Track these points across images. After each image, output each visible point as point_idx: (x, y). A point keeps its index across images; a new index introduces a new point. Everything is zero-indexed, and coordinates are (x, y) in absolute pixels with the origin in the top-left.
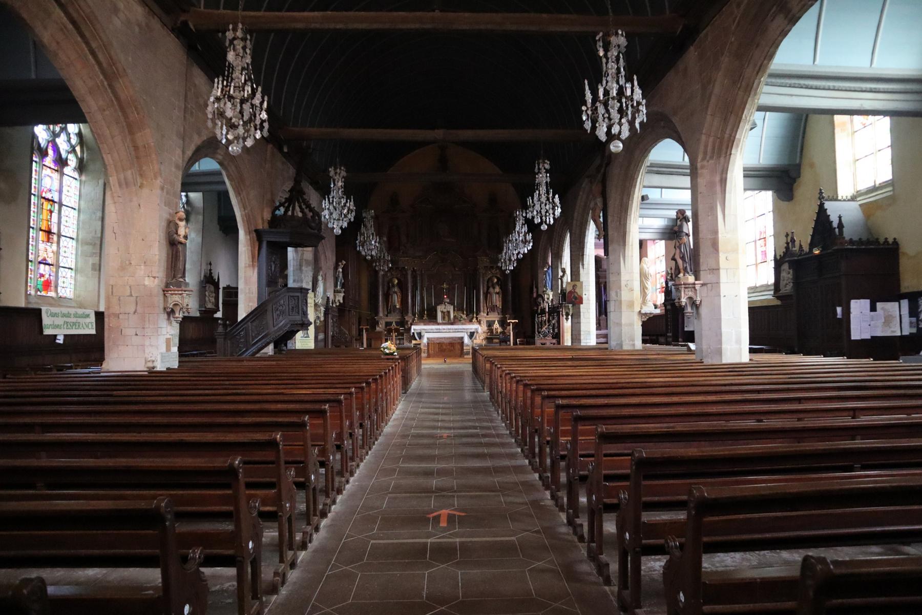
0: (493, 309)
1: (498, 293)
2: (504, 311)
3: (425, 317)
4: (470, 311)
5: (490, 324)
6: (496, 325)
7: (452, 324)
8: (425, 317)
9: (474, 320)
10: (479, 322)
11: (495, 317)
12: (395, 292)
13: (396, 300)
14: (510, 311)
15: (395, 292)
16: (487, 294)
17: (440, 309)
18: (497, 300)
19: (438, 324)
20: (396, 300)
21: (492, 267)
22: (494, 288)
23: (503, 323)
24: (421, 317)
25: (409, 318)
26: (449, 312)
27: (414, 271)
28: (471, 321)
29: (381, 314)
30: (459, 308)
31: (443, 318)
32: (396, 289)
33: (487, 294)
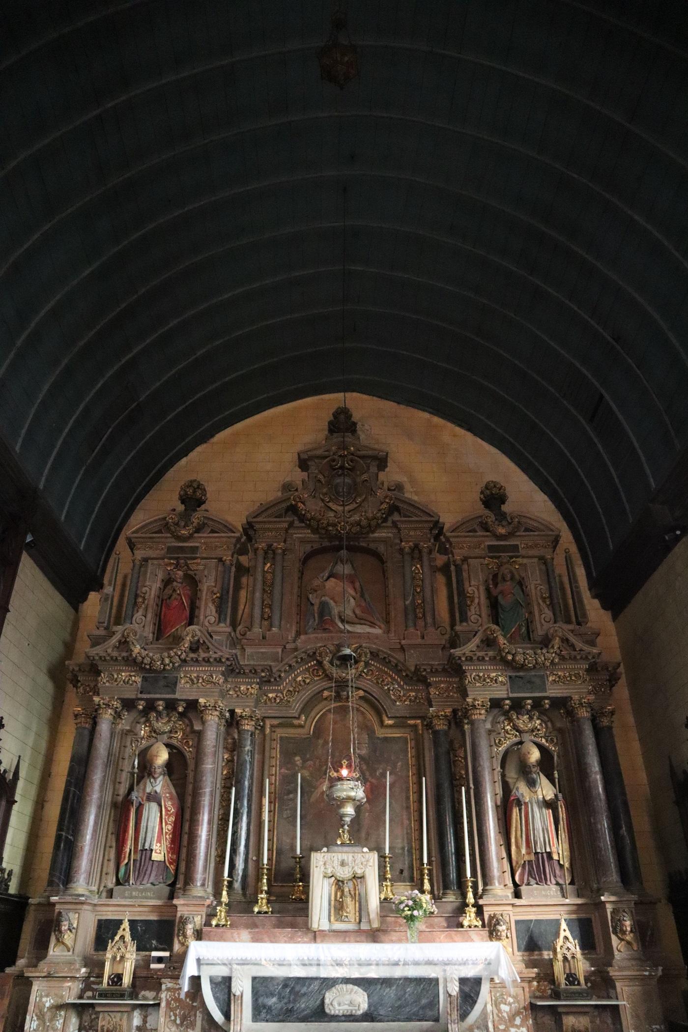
0: (538, 868)
1: (550, 805)
2: (583, 876)
3: (262, 904)
4: (443, 872)
5: (533, 942)
6: (567, 943)
7: (374, 936)
8: (262, 904)
9: (470, 917)
10: (492, 929)
11: (550, 904)
12: (153, 797)
13: (155, 828)
14: (614, 876)
15: (153, 797)
16: (507, 805)
17: (325, 868)
18: (545, 830)
19: (316, 936)
20: (155, 828)
21: (517, 705)
22: (532, 784)
23: (589, 932)
24: (243, 905)
25: (190, 909)
26: (358, 879)
27: (232, 721)
28: (454, 922)
29: (81, 885)
30: (402, 870)
31: (338, 908)
32: (159, 785)
33: (507, 805)
